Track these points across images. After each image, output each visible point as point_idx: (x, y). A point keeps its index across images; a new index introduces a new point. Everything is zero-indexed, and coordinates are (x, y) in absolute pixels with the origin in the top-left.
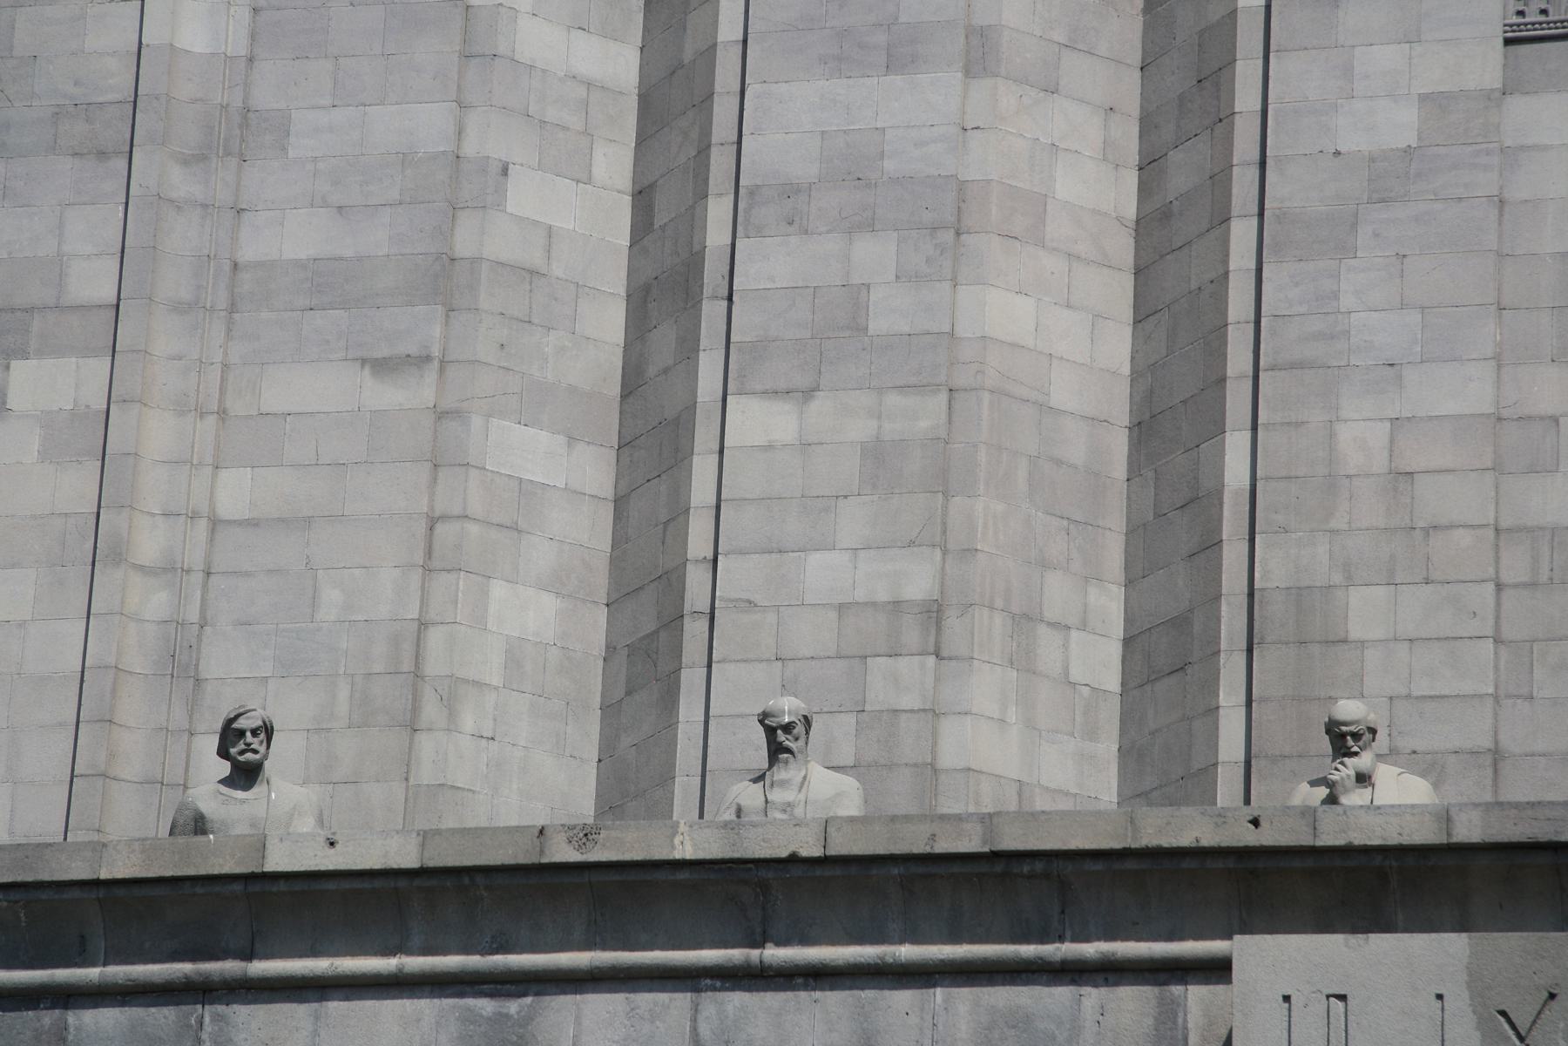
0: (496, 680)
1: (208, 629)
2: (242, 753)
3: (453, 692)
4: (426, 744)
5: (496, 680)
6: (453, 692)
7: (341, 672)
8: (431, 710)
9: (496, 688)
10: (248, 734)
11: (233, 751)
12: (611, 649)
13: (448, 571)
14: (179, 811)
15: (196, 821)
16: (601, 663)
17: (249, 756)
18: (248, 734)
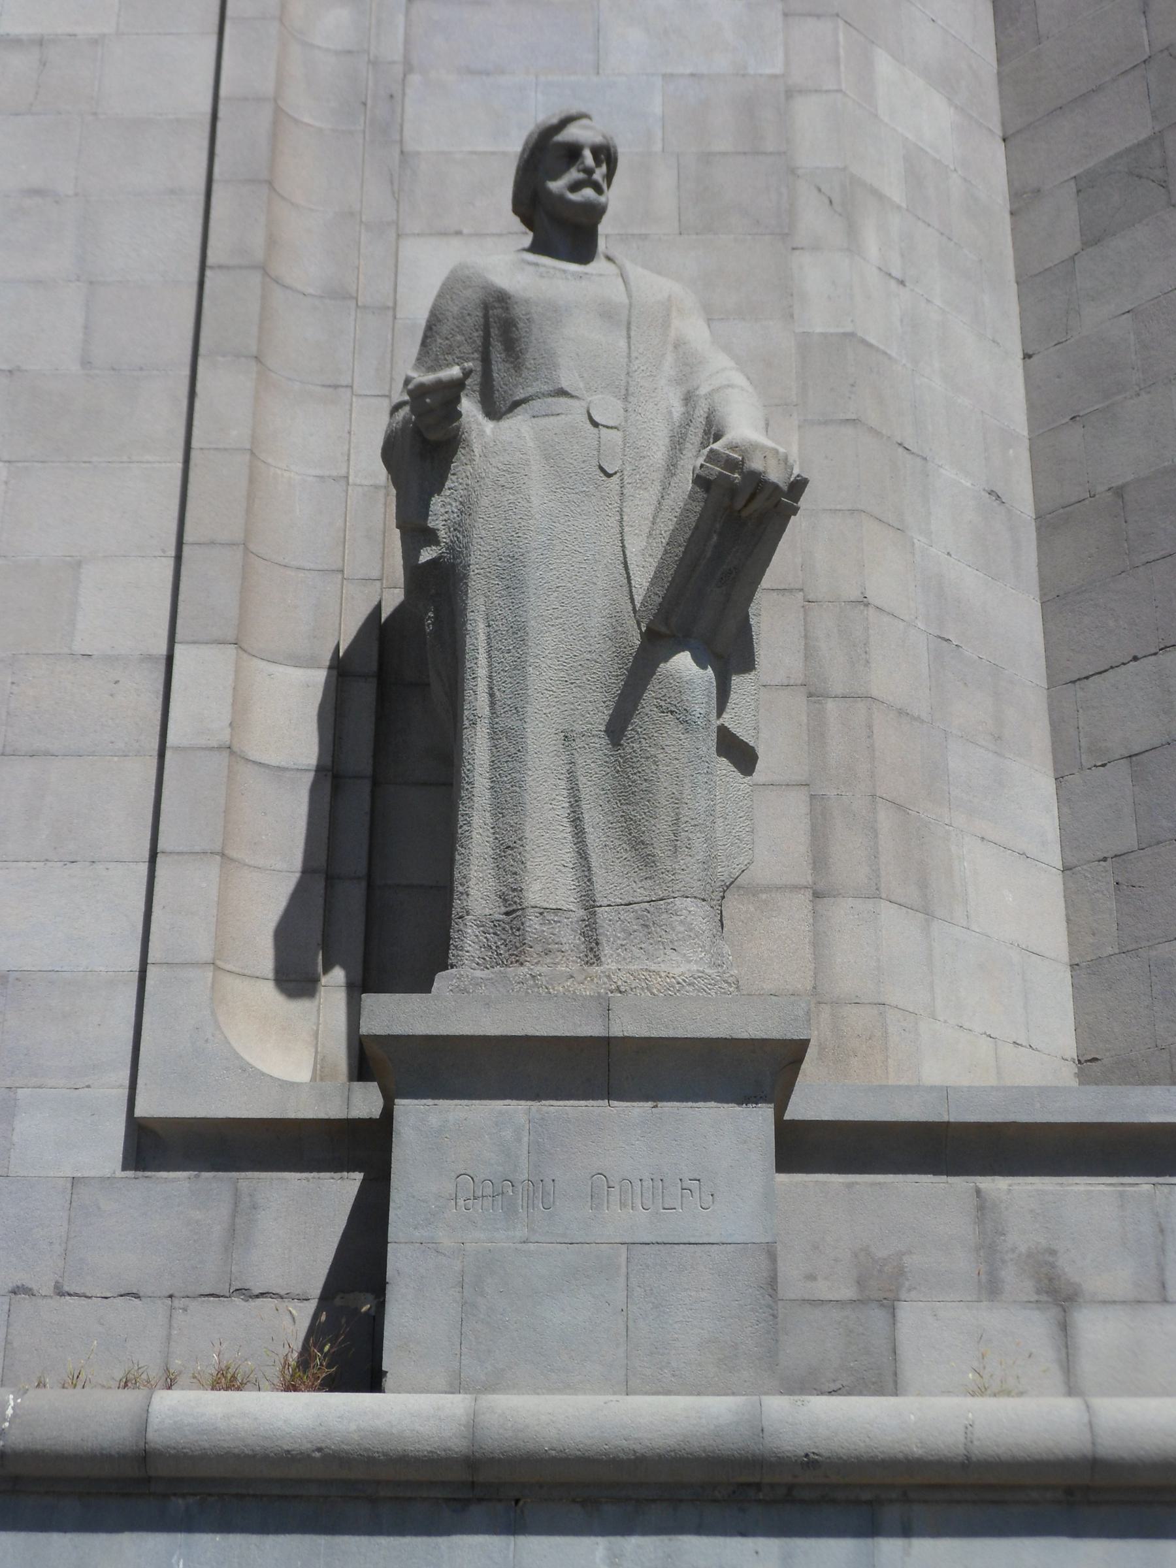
0: (896, 193)
1: (415, 79)
2: (575, 187)
3: (848, 200)
4: (812, 274)
5: (896, 193)
6: (848, 200)
7: (658, 147)
8: (812, 218)
9: (899, 207)
10: (587, 154)
11: (556, 186)
12: (1023, 199)
13: (818, 16)
14: (448, 290)
15: (486, 307)
16: (1007, 216)
17: (588, 193)
18: (587, 154)
